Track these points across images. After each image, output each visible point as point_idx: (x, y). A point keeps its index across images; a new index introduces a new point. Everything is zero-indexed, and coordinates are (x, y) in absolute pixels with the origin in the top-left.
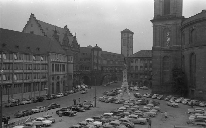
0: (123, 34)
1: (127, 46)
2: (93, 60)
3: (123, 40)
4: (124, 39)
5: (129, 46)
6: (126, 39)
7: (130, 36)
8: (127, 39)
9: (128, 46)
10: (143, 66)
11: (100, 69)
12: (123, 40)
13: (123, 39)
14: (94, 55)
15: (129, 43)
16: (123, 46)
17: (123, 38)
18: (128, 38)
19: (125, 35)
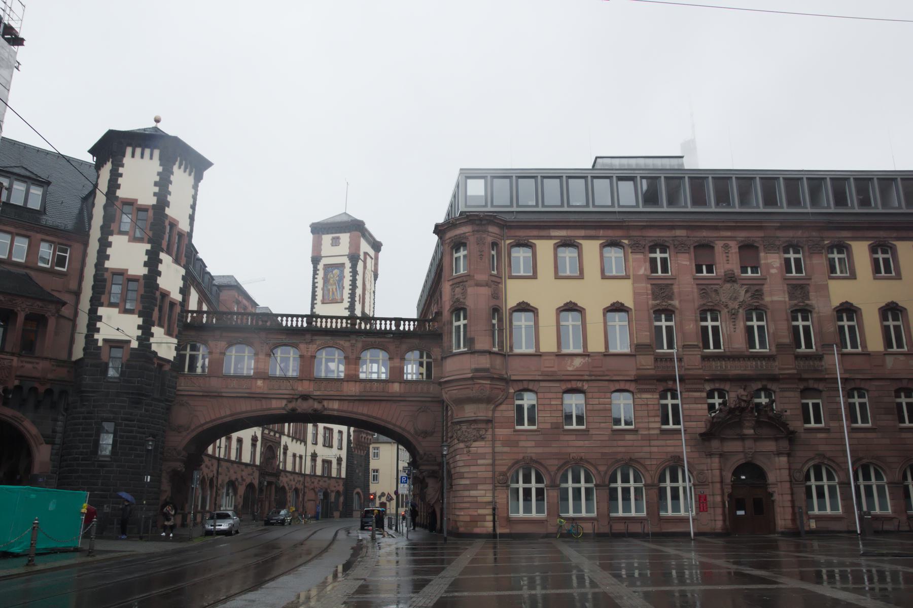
0: (327, 239)
1: (347, 305)
2: (104, 244)
3: (321, 273)
4: (327, 267)
6: (343, 265)
7: (366, 254)
8: (348, 265)
10: (629, 303)
12: (321, 273)
13: (320, 267)
14: (120, 193)
15: (359, 291)
16: (323, 303)
17: (324, 261)
18: (354, 258)
19: (336, 242)
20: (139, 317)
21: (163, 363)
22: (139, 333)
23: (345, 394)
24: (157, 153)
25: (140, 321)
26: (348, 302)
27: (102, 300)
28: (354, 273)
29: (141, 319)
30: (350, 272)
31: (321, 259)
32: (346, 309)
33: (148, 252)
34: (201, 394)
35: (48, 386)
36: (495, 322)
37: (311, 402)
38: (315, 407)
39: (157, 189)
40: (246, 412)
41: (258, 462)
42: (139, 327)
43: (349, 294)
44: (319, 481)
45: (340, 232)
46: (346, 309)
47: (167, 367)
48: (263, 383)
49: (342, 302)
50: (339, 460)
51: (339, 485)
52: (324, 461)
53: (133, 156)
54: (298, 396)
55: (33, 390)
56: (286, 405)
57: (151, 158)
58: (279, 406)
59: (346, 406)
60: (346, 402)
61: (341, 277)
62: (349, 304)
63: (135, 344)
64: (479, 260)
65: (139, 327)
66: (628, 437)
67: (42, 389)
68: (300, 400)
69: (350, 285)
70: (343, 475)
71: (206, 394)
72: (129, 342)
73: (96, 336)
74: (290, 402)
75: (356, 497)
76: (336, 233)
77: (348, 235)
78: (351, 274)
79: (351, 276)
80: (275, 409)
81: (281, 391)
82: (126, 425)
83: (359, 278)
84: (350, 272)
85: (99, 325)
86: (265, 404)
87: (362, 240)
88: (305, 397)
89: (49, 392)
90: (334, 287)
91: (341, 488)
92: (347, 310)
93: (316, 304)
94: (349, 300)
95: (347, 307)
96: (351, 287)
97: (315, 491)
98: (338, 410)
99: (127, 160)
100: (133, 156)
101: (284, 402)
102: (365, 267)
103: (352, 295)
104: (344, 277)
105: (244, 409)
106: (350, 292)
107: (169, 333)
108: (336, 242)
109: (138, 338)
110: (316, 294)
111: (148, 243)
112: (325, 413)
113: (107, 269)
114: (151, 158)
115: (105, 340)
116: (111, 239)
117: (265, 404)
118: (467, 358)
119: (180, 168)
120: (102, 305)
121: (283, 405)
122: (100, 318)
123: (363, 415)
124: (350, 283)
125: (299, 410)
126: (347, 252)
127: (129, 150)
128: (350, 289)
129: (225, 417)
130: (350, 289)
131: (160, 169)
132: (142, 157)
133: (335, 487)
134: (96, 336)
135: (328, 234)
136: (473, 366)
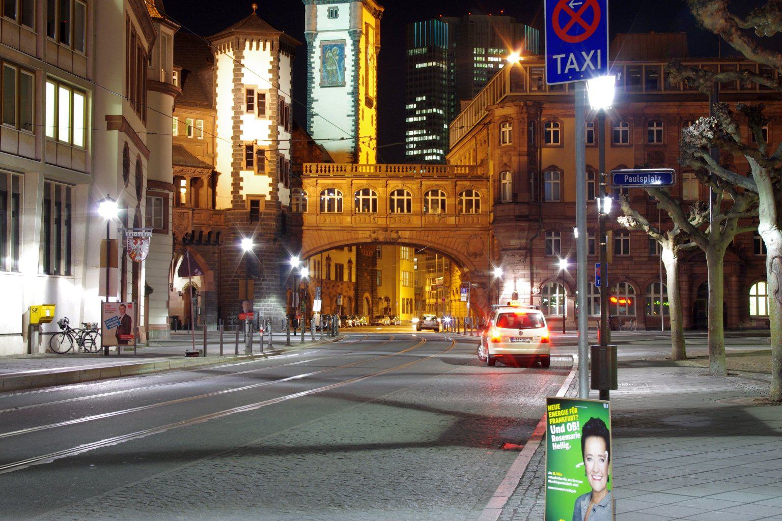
1: (350, 89)
2: (237, 124)
5: (362, 97)
7: (367, 25)
8: (349, 42)
9: (355, 93)
11: (510, 110)
19: (333, 14)
20: (269, 177)
22: (271, 189)
23: (414, 226)
24: (268, 44)
25: (270, 180)
26: (351, 86)
27: (242, 166)
28: (357, 51)
29: (271, 179)
30: (352, 50)
31: (317, 34)
32: (349, 94)
33: (270, 127)
36: (532, 181)
39: (271, 76)
40: (340, 241)
42: (270, 185)
43: (352, 76)
44: (333, 286)
45: (339, 2)
46: (349, 94)
49: (344, 86)
50: (350, 262)
51: (350, 290)
52: (336, 265)
53: (251, 49)
56: (370, 235)
57: (264, 50)
58: (364, 236)
61: (342, 57)
62: (352, 88)
63: (268, 198)
64: (521, 136)
65: (270, 185)
66: (625, 263)
68: (380, 232)
69: (353, 66)
70: (354, 280)
72: (264, 196)
73: (241, 192)
75: (365, 301)
76: (334, 2)
77: (347, 5)
78: (353, 53)
79: (353, 55)
80: (362, 238)
81: (364, 225)
83: (362, 56)
84: (352, 50)
85: (242, 184)
87: (365, 11)
89: (210, 233)
90: (334, 68)
91: (352, 293)
92: (351, 96)
93: (314, 88)
94: (353, 83)
95: (351, 92)
96: (354, 68)
97: (330, 296)
99: (246, 52)
100: (251, 49)
102: (367, 42)
103: (356, 78)
104: (346, 56)
105: (338, 239)
106: (353, 74)
107: (286, 186)
108: (333, 14)
109: (270, 193)
110: (313, 76)
111: (270, 119)
112: (399, 241)
113: (242, 141)
114: (264, 50)
115: (248, 196)
116: (242, 118)
118: (512, 206)
119: (283, 53)
120: (242, 169)
121: (368, 236)
122: (242, 179)
124: (353, 63)
126: (347, 25)
127: (247, 43)
128: (353, 71)
129: (324, 245)
130: (353, 71)
131: (272, 59)
132: (257, 49)
133: (347, 292)
134: (241, 192)
135: (324, 3)
136: (517, 214)
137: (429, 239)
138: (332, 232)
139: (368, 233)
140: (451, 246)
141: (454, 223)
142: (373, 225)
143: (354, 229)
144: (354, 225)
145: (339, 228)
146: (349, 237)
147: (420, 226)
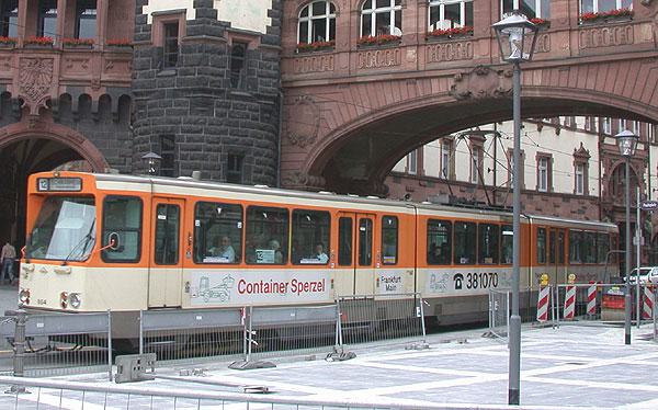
21: (246, 38)
34: (326, 82)
35: (103, 91)
37: (492, 77)
38: (502, 86)
41: (594, 189)
47: (254, 45)
48: (417, 52)
54: (471, 70)
55: (85, 98)
59: (557, 80)
60: (555, 72)
63: (191, 15)
67: (95, 96)
68: (474, 76)
71: (332, 82)
74: (459, 80)
82: (189, 140)
86: (421, 90)
88: (482, 71)
89: (105, 99)
98: (541, 88)
101: (451, 82)
115: (155, 15)
117: (421, 90)
123: (587, 92)
125: (475, 94)
134: (147, 10)
137: (591, 86)
138: (379, 86)
139: (451, 82)
140: (645, 100)
141: (650, 37)
142: (463, 63)
143: (422, 75)
144: (421, 68)
145: (390, 77)
146: (413, 96)
147: (568, 55)
